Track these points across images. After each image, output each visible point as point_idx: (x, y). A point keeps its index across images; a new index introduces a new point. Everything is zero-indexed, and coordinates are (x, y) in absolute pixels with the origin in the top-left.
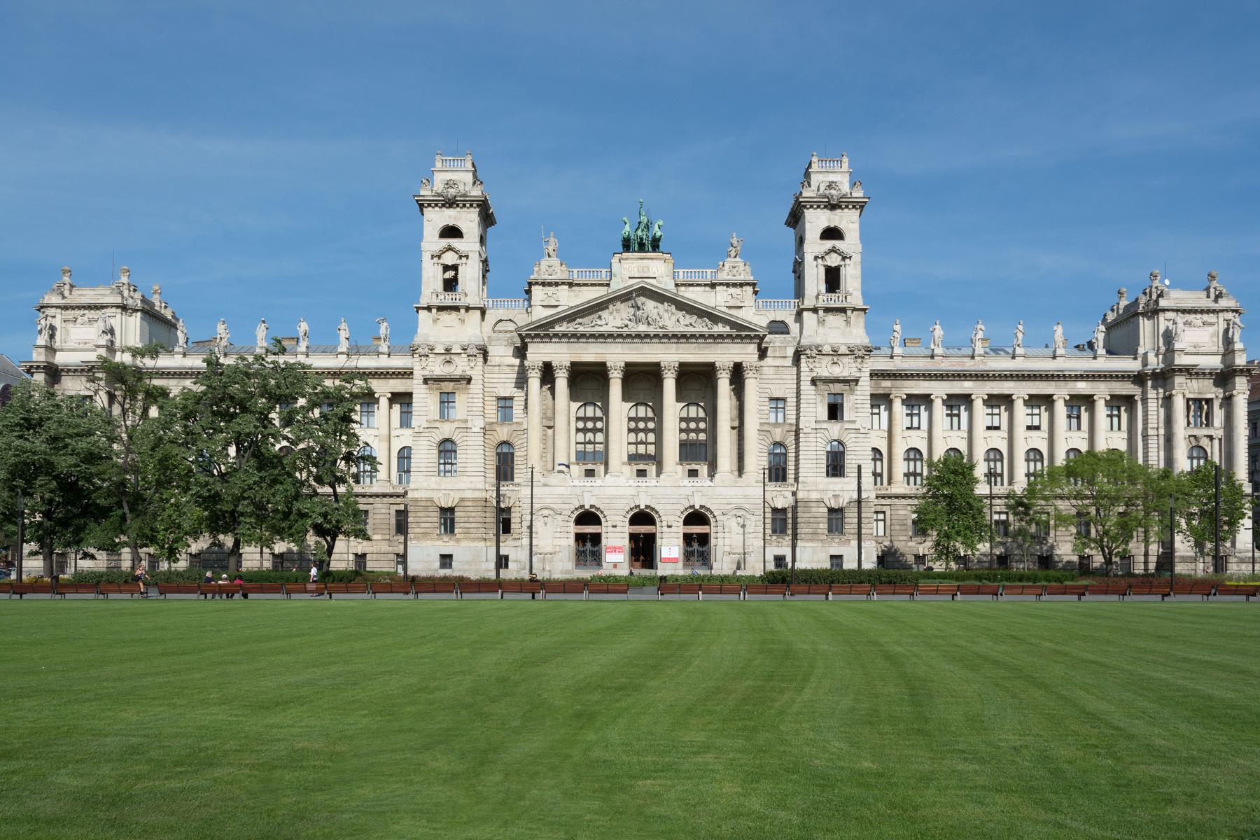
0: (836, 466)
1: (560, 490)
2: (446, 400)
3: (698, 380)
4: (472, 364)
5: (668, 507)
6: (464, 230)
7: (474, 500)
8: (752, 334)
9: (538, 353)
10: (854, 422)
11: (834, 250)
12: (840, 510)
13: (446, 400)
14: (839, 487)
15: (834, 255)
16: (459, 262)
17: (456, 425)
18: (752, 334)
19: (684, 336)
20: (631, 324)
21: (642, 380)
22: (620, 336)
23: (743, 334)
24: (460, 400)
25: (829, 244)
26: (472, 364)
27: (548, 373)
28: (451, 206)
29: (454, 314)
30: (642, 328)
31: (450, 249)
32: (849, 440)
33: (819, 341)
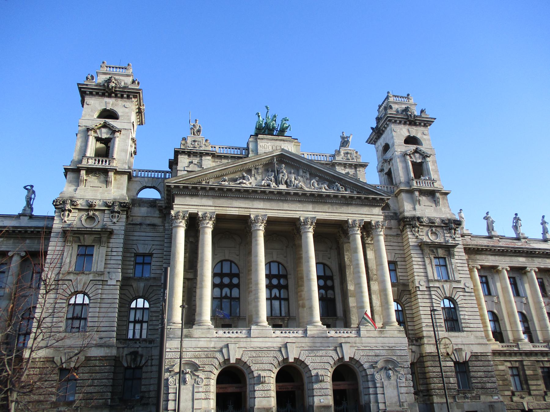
0: (453, 321)
1: (203, 343)
2: (85, 254)
3: (333, 236)
4: (115, 220)
5: (318, 359)
6: (120, 114)
7: (102, 359)
8: (378, 197)
9: (183, 206)
10: (459, 282)
11: (416, 151)
12: (465, 363)
13: (85, 254)
14: (459, 341)
15: (417, 155)
16: (111, 136)
17: (91, 277)
18: (378, 197)
19: (320, 196)
20: (273, 185)
21: (284, 234)
22: (264, 192)
23: (371, 196)
24: (99, 254)
25: (412, 147)
26: (115, 220)
27: (194, 223)
28: (110, 96)
29: (102, 177)
30: (283, 187)
31: (105, 126)
32: (459, 298)
33: (418, 214)
